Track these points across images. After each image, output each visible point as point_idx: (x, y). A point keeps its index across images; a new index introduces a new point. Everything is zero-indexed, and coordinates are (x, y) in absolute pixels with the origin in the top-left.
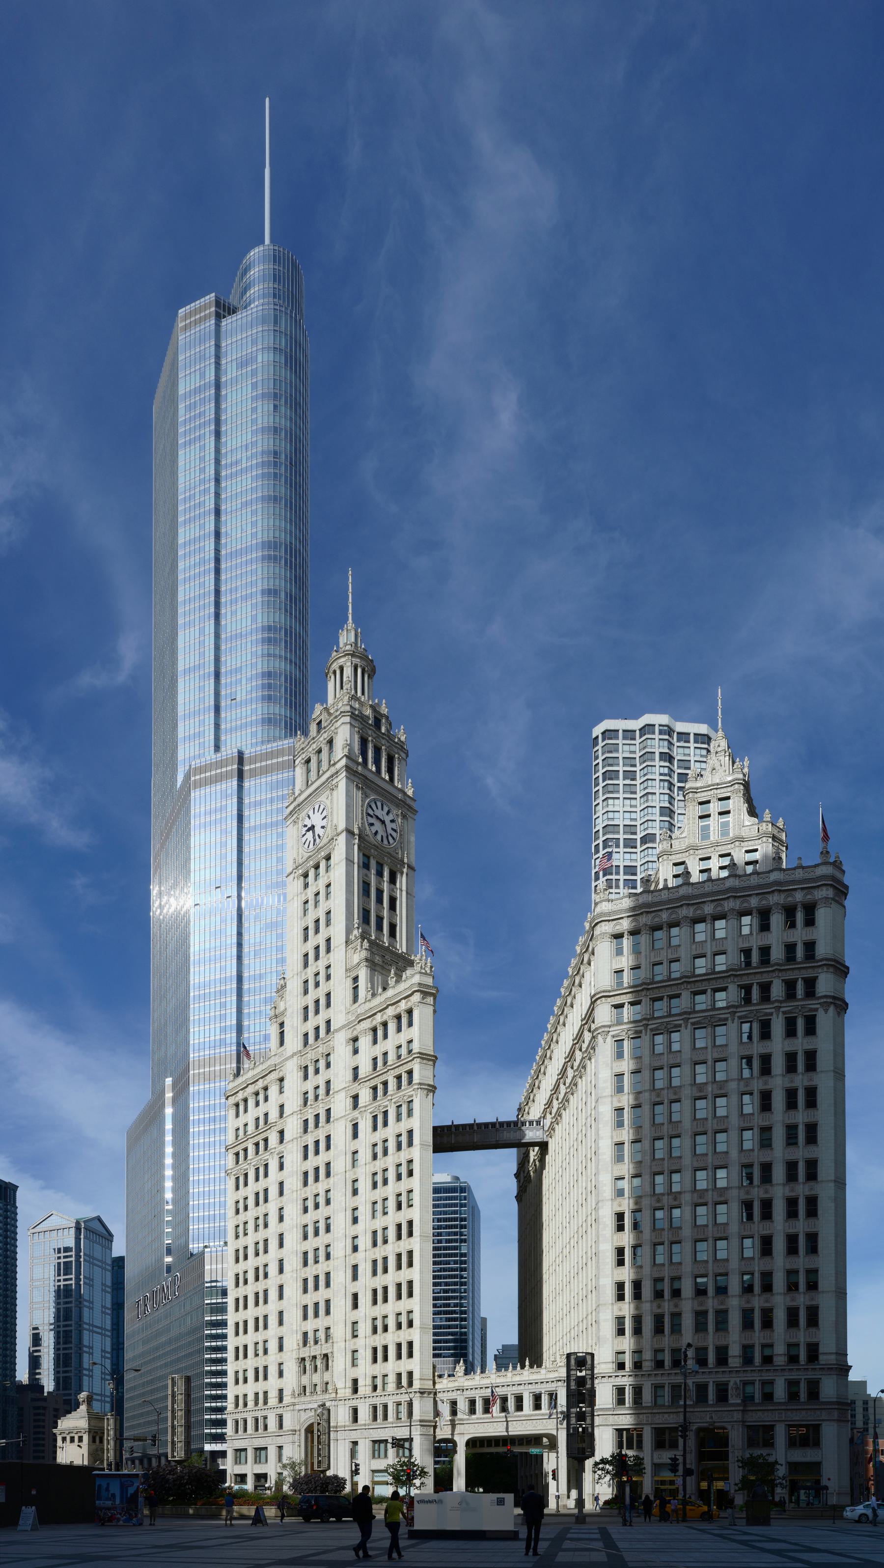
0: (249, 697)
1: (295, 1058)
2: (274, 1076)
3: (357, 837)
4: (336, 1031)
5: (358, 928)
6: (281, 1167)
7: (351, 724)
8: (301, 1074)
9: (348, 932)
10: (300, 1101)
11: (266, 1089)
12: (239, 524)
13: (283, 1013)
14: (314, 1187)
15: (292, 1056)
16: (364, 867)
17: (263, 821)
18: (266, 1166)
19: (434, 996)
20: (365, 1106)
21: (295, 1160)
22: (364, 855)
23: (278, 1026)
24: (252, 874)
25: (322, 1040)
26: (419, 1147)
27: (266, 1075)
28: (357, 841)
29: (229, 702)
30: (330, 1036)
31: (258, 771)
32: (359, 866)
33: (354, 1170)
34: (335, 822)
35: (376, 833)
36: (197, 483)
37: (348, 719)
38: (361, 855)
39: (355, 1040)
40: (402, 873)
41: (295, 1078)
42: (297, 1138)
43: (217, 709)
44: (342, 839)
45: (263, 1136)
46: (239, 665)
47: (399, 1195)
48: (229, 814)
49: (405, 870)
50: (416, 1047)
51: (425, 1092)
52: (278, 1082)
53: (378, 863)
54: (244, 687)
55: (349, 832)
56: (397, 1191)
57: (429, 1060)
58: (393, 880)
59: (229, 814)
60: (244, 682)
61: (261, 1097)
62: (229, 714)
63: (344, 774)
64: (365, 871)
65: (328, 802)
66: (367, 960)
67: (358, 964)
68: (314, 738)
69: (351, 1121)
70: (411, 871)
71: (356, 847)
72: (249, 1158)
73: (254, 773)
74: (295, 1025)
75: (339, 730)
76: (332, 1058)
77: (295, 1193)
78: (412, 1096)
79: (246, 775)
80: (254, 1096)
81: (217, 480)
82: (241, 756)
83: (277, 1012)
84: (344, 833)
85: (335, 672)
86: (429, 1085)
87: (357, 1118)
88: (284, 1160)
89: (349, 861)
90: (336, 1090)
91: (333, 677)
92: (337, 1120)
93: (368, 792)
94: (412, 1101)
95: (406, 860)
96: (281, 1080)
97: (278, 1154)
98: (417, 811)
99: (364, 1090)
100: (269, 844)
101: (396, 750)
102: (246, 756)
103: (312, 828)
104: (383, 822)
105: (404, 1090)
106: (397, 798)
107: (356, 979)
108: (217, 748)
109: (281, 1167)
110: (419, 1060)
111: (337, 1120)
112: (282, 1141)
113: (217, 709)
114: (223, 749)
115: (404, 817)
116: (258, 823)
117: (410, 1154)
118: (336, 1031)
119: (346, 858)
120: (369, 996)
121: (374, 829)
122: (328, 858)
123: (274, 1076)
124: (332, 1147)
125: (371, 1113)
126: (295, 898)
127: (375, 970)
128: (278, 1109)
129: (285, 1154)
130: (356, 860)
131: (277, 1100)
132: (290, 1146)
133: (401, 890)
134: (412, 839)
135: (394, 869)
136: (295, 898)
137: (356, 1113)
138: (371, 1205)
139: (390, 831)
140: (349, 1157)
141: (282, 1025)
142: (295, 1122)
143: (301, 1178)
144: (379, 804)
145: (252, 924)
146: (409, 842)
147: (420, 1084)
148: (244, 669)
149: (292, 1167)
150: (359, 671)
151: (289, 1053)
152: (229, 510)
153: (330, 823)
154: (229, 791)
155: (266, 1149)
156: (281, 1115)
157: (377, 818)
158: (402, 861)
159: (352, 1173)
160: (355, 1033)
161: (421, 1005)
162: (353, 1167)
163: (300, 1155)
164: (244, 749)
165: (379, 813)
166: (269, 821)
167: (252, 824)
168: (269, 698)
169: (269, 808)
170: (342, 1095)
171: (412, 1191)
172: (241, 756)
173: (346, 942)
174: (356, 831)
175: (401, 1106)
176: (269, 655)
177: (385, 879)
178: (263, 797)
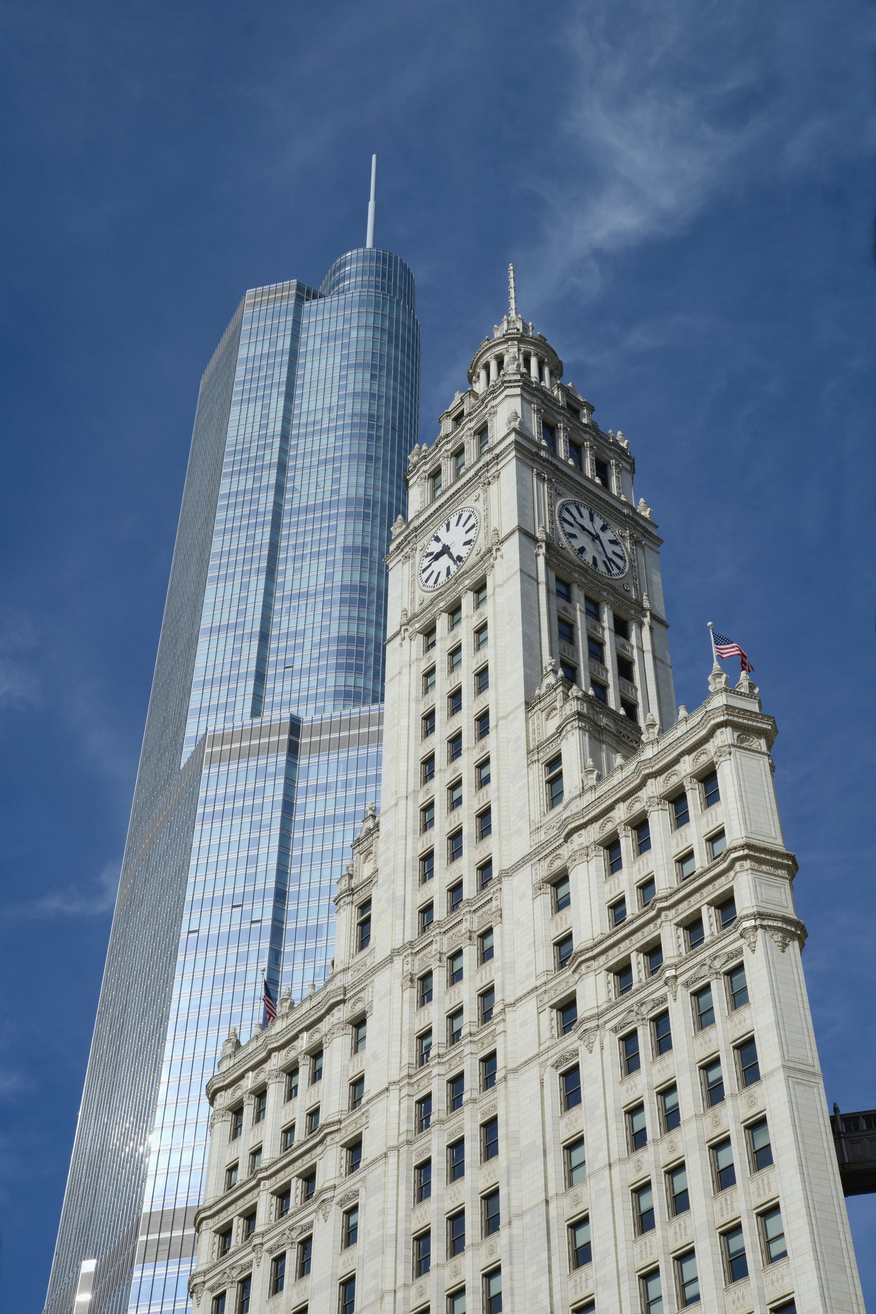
0: (314, 664)
1: (398, 961)
2: (343, 1014)
3: (544, 545)
4: (507, 873)
5: (555, 672)
6: (350, 1236)
7: (523, 398)
8: (413, 993)
9: (530, 684)
10: (409, 1054)
11: (316, 1053)
12: (313, 480)
13: (370, 881)
14: (447, 1271)
15: (390, 960)
16: (559, 593)
17: (330, 812)
18: (306, 1244)
19: (768, 736)
20: (599, 1016)
21: (391, 1205)
22: (558, 580)
23: (355, 910)
24: (304, 888)
25: (470, 902)
26: (781, 1075)
27: (320, 1019)
28: (543, 551)
29: (280, 670)
30: (492, 889)
31: (325, 745)
32: (548, 591)
33: (572, 1191)
34: (494, 524)
35: (582, 550)
36: (255, 438)
37: (518, 391)
38: (552, 575)
39: (560, 880)
40: (641, 625)
41: (397, 1005)
42: (397, 1148)
43: (260, 677)
44: (512, 550)
45: (301, 1166)
46: (301, 627)
47: (732, 1231)
48: (268, 800)
49: (647, 620)
50: (735, 836)
51: (778, 937)
52: (350, 1029)
53: (587, 599)
54: (307, 652)
55: (526, 535)
56: (724, 1219)
57: (777, 865)
58: (621, 629)
59: (268, 800)
60: (307, 646)
61: (304, 1073)
62: (279, 685)
63: (513, 453)
64: (563, 602)
65: (479, 506)
66: (579, 715)
67: (560, 731)
68: (447, 436)
69: (556, 1066)
70: (656, 626)
71: (541, 561)
72: (258, 1229)
73: (314, 748)
74: (400, 893)
75: (499, 409)
76: (496, 940)
77: (389, 1299)
78: (739, 952)
79: (303, 750)
80: (284, 1078)
81: (285, 437)
82: (295, 726)
83: (354, 882)
84: (516, 535)
85: (487, 367)
86: (785, 920)
87: (575, 1053)
88: (360, 1218)
89: (527, 576)
90: (510, 1000)
91: (483, 374)
92: (515, 1070)
93: (562, 489)
94: (740, 967)
95: (646, 604)
96: (359, 1022)
97: (341, 1203)
98: (662, 541)
99: (590, 980)
100: (338, 845)
101: (611, 454)
102: (305, 725)
103: (446, 550)
104: (596, 538)
105: (713, 943)
106: (622, 513)
107: (555, 762)
108: (256, 712)
109: (350, 1236)
110: (748, 864)
111: (515, 1070)
112: (353, 1165)
113: (260, 677)
114: (267, 713)
115: (636, 542)
116: (320, 814)
117: (752, 1103)
118: (507, 873)
119: (521, 571)
120: (592, 780)
121: (577, 544)
122: (480, 588)
123: (343, 1014)
124: (502, 1145)
125: (615, 1030)
126: (406, 670)
127: (602, 742)
128: (346, 1090)
129: (361, 1201)
130: (542, 577)
131: (344, 1069)
132: (377, 1171)
133: (641, 650)
134: (657, 578)
135: (623, 615)
136: (406, 670)
137: (572, 1040)
138: (636, 1283)
139: (611, 556)
140: (556, 1160)
141: (366, 906)
142: (394, 1108)
143: (407, 1251)
144: (585, 512)
145: (299, 966)
146: (649, 582)
147: (760, 915)
148: (309, 633)
149: (383, 1225)
150: (534, 362)
151: (380, 957)
152: (299, 466)
153: (482, 536)
154: (271, 769)
155: (308, 1195)
156: (355, 1102)
157: (583, 528)
158: (639, 604)
159: (566, 1202)
160: (558, 864)
161: (737, 753)
162: (570, 1183)
163: (407, 1189)
164: (302, 715)
165: (586, 522)
166: (340, 811)
167: (310, 816)
168: (348, 668)
169: (341, 794)
170: (530, 1006)
171: (774, 1209)
172: (295, 726)
173: (527, 703)
174: (540, 535)
175: (707, 988)
176: (350, 618)
177: (606, 624)
178: (332, 779)
